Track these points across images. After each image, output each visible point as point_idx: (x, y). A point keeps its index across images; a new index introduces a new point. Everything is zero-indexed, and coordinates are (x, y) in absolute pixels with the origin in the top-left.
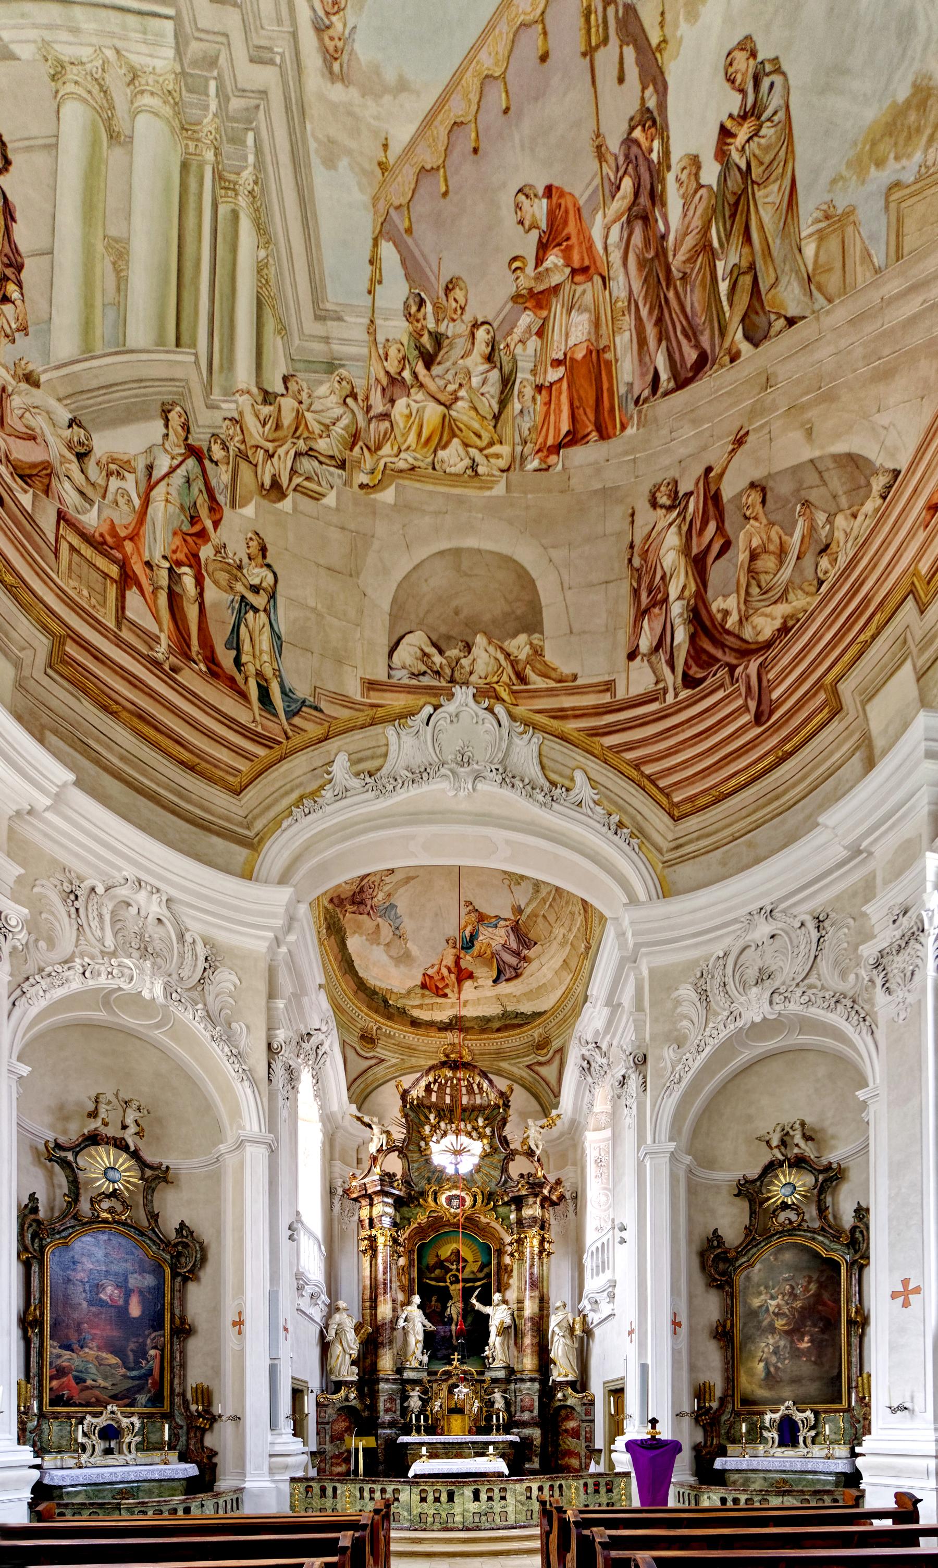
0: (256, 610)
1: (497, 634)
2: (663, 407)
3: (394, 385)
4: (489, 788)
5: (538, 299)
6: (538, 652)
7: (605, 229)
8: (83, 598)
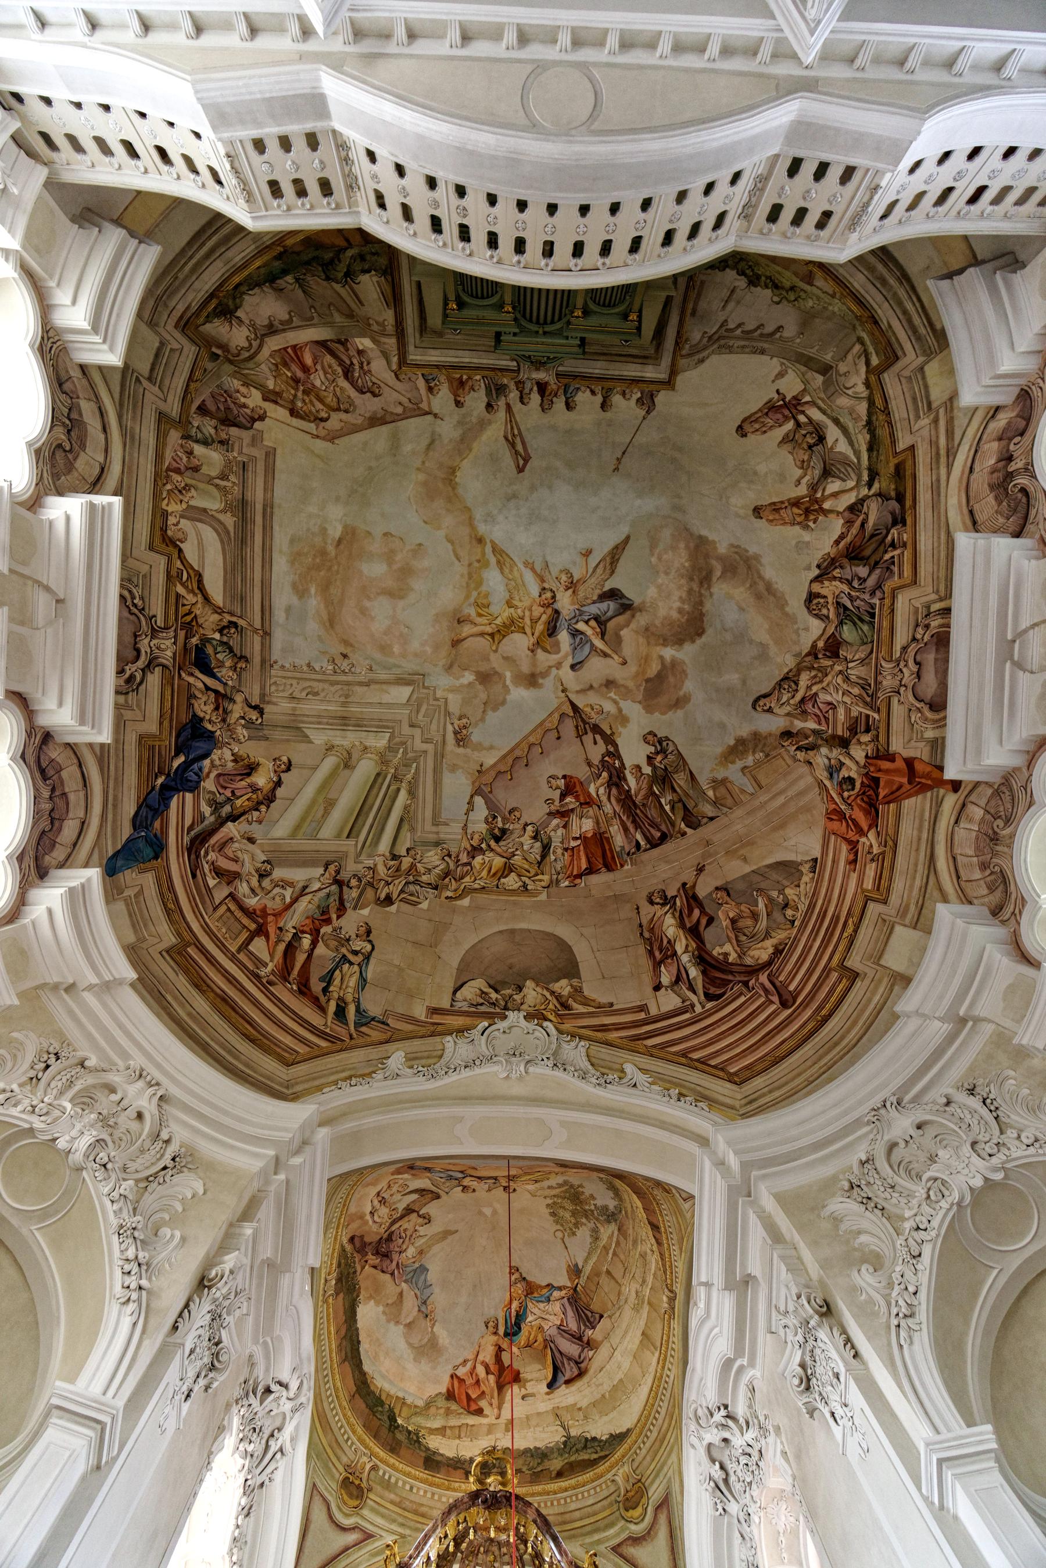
0: (351, 964)
1: (543, 979)
2: (645, 856)
3: (475, 851)
4: (542, 1070)
5: (564, 814)
6: (578, 991)
7: (596, 789)
8: (222, 932)
